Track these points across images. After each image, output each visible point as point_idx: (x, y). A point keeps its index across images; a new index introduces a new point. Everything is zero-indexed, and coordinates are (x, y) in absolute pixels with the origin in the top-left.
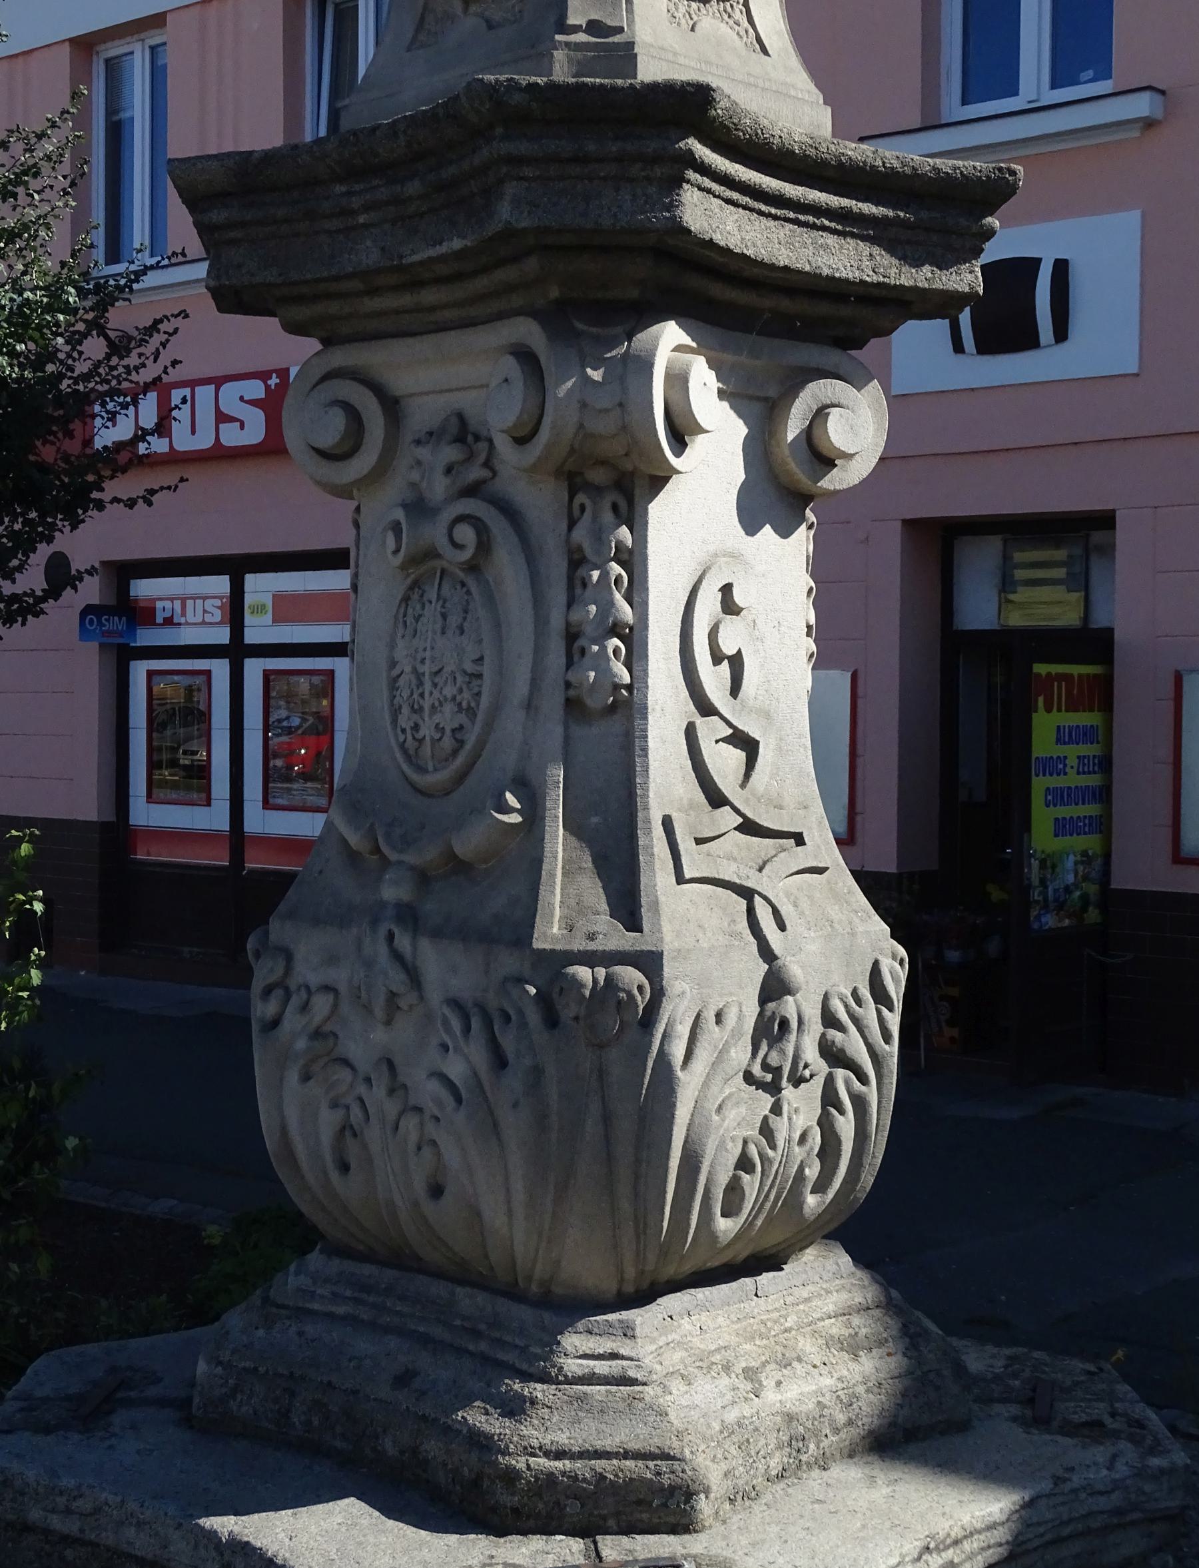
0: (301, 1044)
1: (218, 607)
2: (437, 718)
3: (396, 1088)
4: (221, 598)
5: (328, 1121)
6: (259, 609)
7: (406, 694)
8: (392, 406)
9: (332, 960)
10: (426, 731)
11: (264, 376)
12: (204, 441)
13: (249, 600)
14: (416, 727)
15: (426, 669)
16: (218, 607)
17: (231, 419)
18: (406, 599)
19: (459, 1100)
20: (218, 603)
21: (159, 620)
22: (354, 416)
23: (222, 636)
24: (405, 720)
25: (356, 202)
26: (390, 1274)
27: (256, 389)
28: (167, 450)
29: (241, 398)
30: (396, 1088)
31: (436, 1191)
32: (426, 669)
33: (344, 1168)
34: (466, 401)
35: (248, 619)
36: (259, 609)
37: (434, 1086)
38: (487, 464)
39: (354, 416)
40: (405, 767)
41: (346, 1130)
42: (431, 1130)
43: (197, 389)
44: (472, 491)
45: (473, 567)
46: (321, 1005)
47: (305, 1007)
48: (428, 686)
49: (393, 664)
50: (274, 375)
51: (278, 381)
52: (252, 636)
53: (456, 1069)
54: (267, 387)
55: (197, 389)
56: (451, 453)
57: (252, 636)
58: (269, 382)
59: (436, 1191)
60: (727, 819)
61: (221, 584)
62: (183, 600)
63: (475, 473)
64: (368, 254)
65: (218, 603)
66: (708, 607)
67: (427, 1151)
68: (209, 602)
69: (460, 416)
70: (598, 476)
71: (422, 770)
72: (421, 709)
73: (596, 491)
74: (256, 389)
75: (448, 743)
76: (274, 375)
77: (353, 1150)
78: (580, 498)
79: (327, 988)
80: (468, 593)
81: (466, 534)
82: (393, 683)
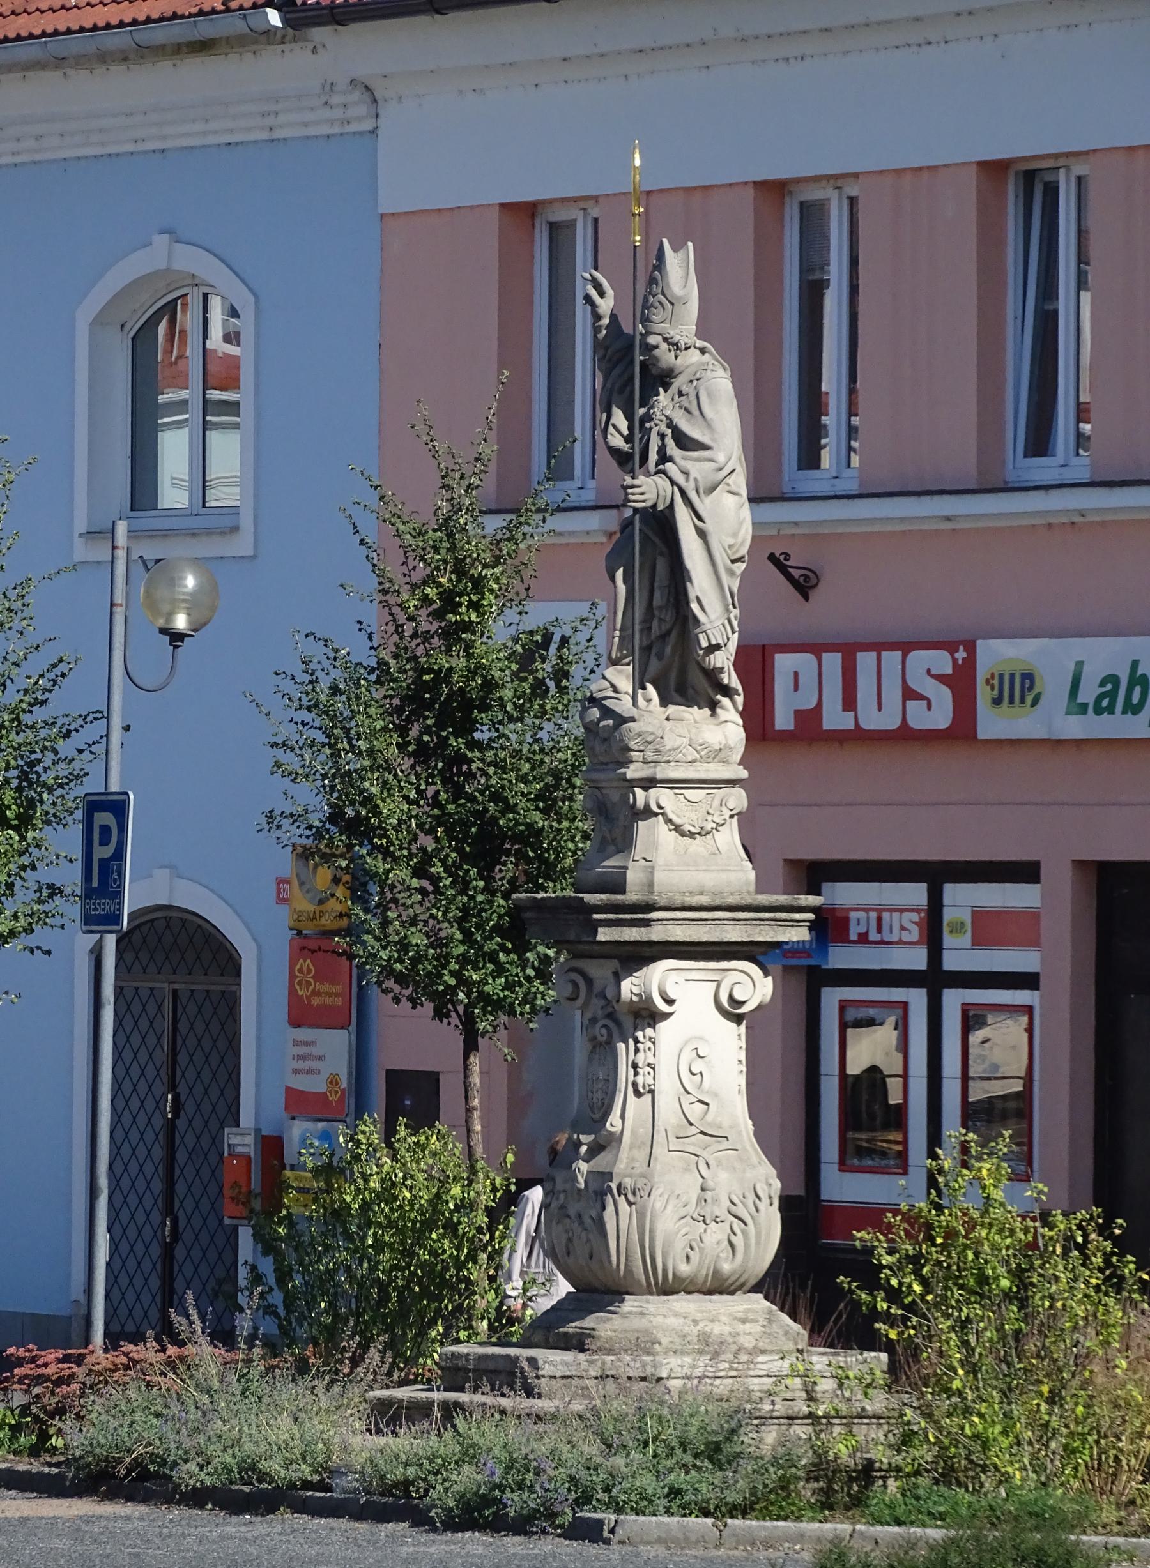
1: (916, 923)
3: (581, 1223)
4: (918, 911)
6: (958, 928)
8: (589, 981)
11: (950, 647)
12: (888, 721)
13: (948, 915)
16: (916, 923)
17: (919, 697)
20: (915, 917)
21: (853, 936)
22: (575, 985)
23: (917, 959)
27: (942, 662)
28: (851, 726)
29: (929, 671)
30: (581, 1223)
35: (948, 940)
36: (958, 928)
39: (575, 985)
41: (570, 1240)
43: (884, 654)
46: (562, 1196)
50: (961, 648)
51: (965, 655)
52: (952, 962)
54: (955, 661)
55: (884, 654)
57: (952, 962)
58: (957, 655)
60: (693, 1130)
61: (916, 894)
62: (880, 911)
65: (915, 917)
66: (688, 1055)
68: (906, 915)
70: (644, 1013)
73: (644, 1018)
74: (942, 662)
76: (961, 648)
81: (604, 1031)
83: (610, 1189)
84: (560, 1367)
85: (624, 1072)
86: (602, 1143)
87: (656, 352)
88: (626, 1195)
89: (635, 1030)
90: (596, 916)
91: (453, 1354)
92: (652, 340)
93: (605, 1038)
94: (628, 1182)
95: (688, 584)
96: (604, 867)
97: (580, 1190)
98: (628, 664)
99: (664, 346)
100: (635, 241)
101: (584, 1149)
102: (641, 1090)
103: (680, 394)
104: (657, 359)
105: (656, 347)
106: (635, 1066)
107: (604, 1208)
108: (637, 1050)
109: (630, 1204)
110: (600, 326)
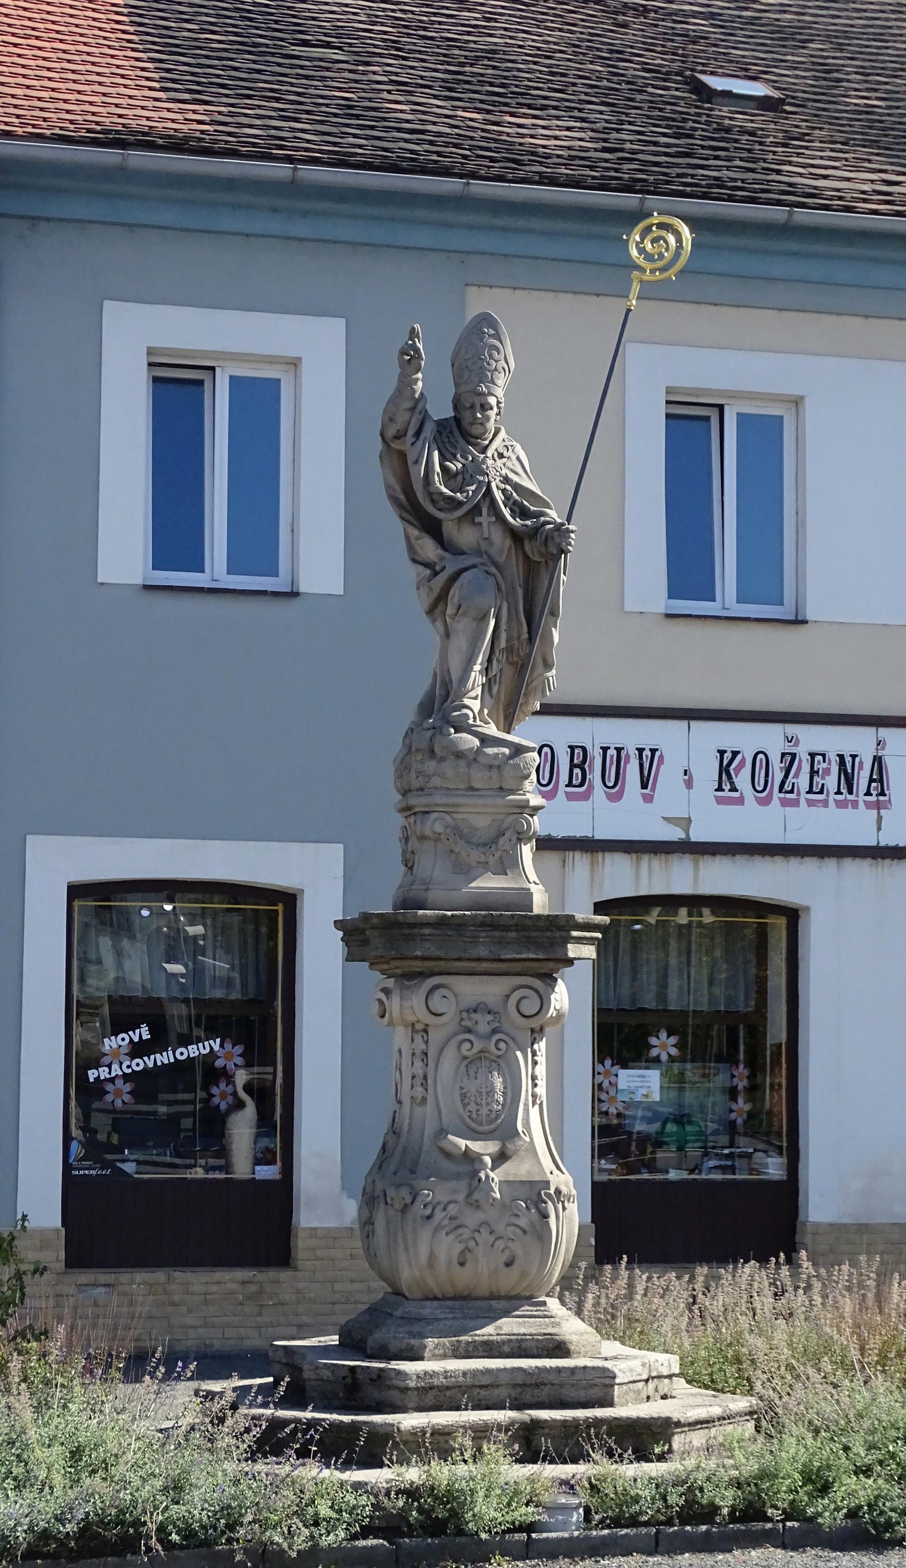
0: (446, 1222)
2: (489, 1107)
5: (459, 1248)
7: (473, 1099)
9: (454, 1192)
10: (484, 1111)
14: (478, 1110)
15: (484, 1090)
18: (467, 1066)
19: (525, 1232)
24: (472, 1107)
25: (483, 934)
26: (458, 1304)
31: (508, 1264)
32: (484, 1090)
33: (462, 1264)
34: (484, 999)
37: (511, 1228)
38: (499, 1022)
40: (473, 1125)
42: (510, 1244)
44: (495, 1031)
45: (499, 1057)
47: (444, 1209)
48: (484, 1096)
49: (462, 1088)
53: (523, 1222)
56: (489, 1017)
59: (508, 1264)
63: (496, 1025)
64: (483, 952)
67: (507, 1253)
69: (483, 1003)
71: (481, 1124)
72: (481, 1104)
75: (493, 1115)
77: (468, 1255)
78: (536, 1035)
79: (456, 1202)
80: (499, 1065)
82: (463, 1096)
83: (549, 1196)
84: (627, 1374)
85: (526, 1083)
86: (508, 1152)
87: (490, 413)
88: (563, 1202)
89: (532, 1044)
90: (575, 934)
91: (426, 1373)
92: (492, 401)
93: (499, 1053)
94: (564, 1190)
95: (553, 629)
96: (472, 888)
97: (494, 1199)
98: (476, 698)
99: (495, 409)
100: (632, 305)
101: (488, 1160)
102: (538, 1102)
103: (501, 456)
104: (488, 419)
105: (491, 409)
106: (534, 1078)
107: (546, 1216)
108: (535, 1063)
109: (564, 1209)
110: (417, 379)
